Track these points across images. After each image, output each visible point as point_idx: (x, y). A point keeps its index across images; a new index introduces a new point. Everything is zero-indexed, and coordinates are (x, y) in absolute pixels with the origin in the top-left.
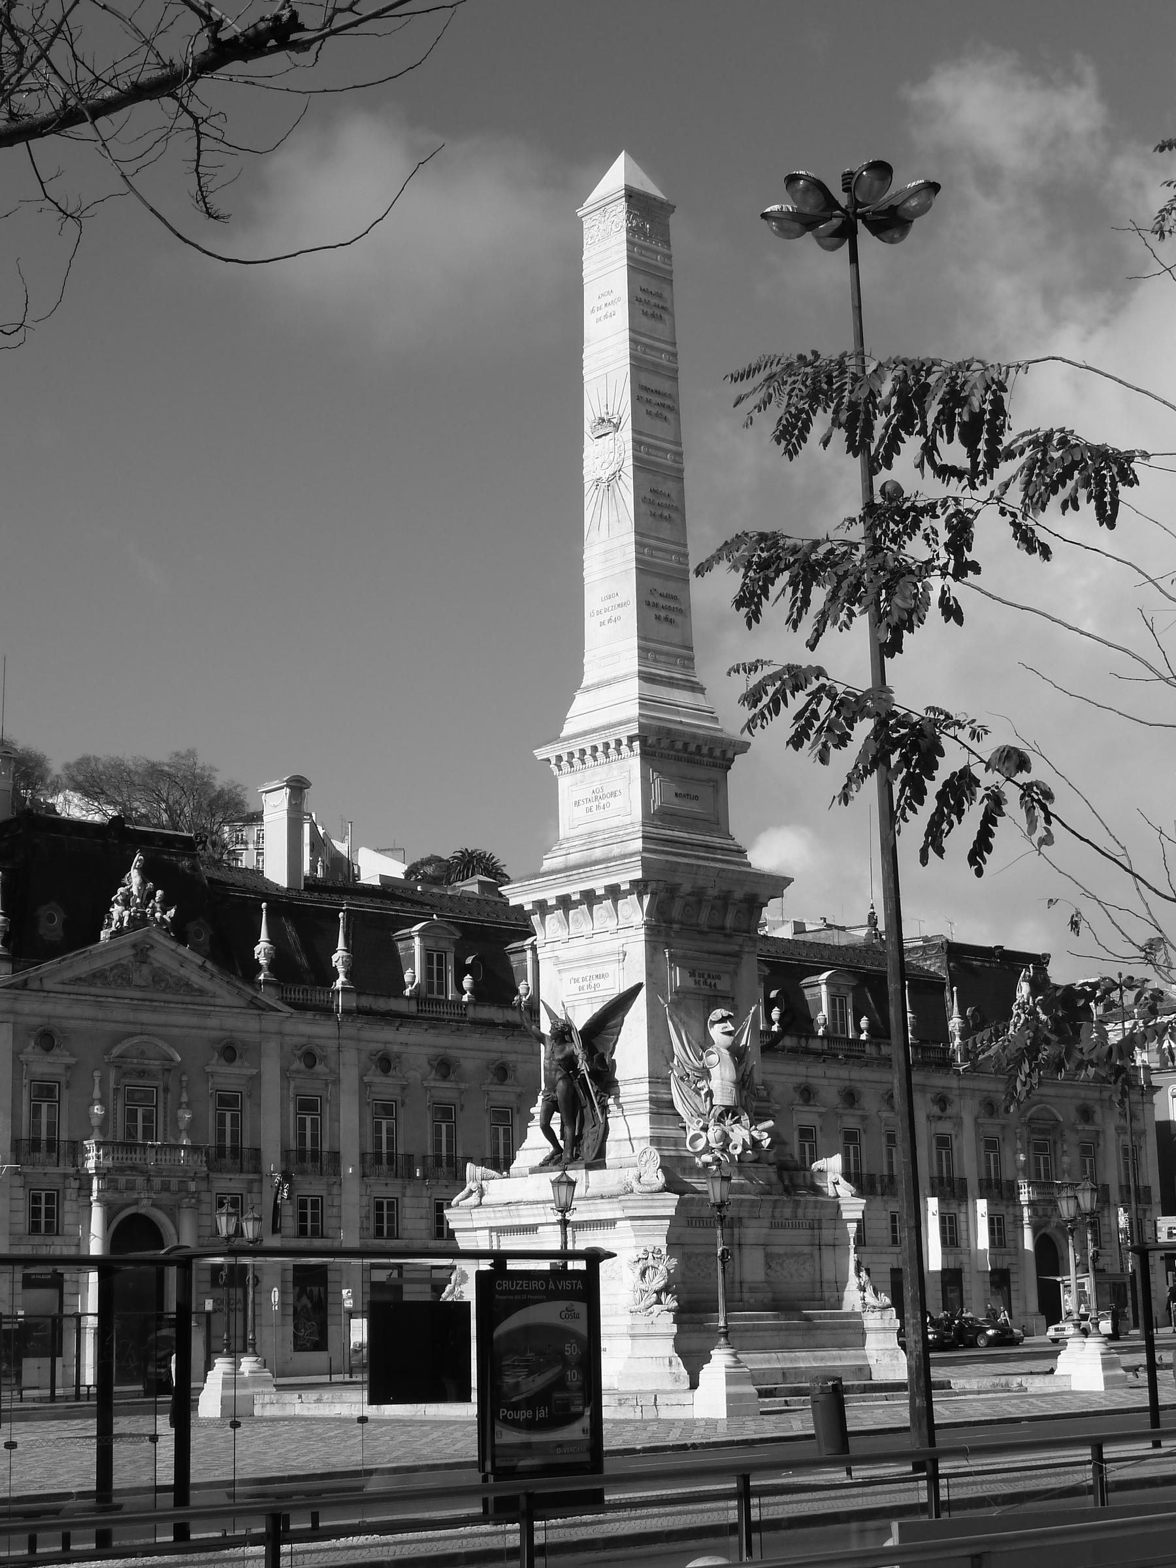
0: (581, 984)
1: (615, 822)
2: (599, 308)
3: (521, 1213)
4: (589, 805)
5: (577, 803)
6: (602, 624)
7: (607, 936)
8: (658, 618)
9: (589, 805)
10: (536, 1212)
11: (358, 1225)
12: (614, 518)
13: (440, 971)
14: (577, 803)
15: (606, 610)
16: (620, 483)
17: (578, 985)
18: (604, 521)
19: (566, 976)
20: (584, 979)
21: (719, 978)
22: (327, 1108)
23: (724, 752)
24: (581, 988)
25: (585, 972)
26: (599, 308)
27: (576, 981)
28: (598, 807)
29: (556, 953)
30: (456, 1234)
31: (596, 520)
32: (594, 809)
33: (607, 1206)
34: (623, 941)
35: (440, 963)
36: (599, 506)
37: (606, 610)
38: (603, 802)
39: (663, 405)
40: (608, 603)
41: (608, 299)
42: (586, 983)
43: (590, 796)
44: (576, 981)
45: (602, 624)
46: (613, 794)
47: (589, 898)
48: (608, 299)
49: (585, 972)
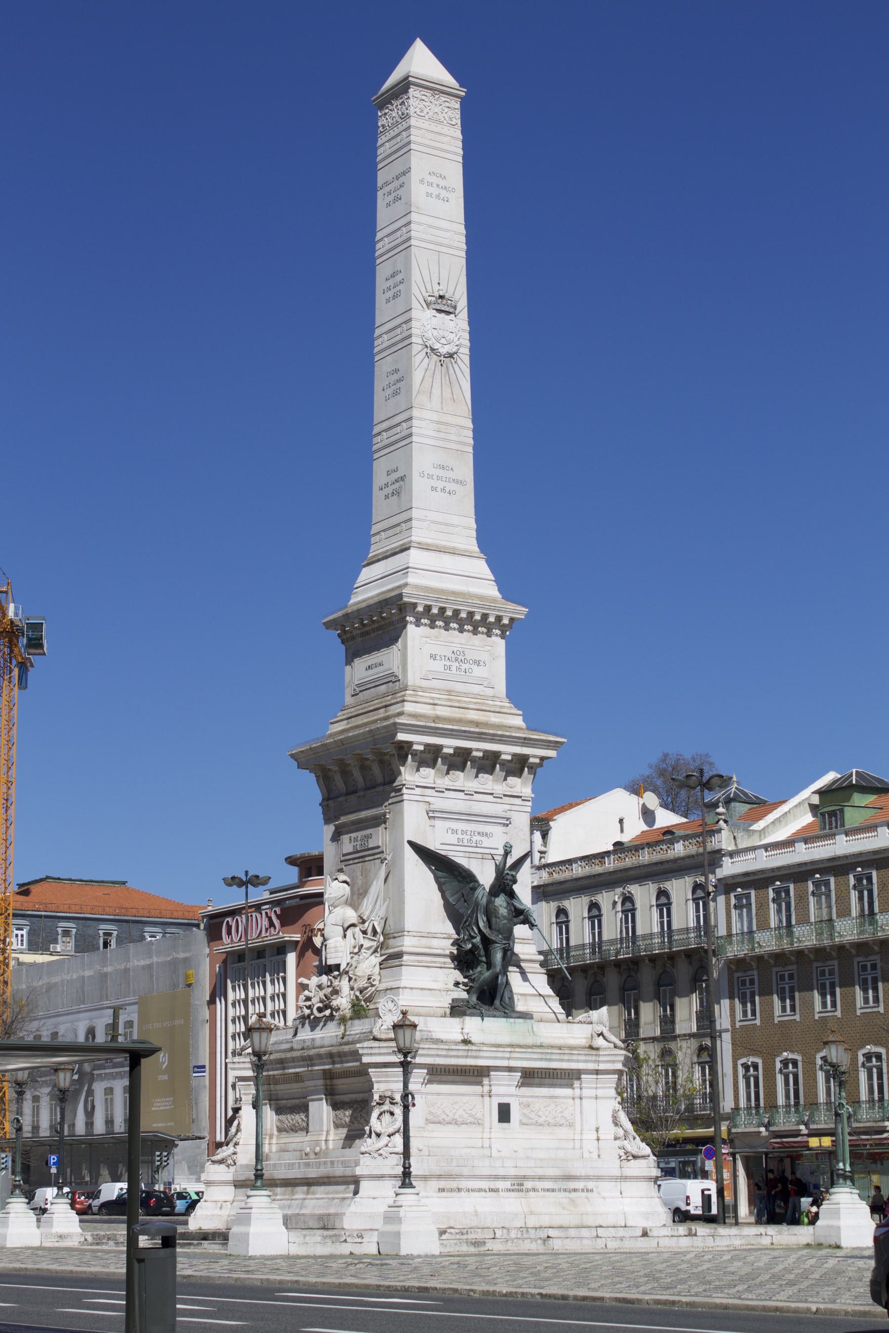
0: (461, 837)
1: (476, 689)
3: (481, 1054)
4: (448, 663)
5: (433, 657)
6: (434, 489)
7: (490, 798)
9: (448, 663)
10: (500, 1055)
12: (447, 393)
14: (433, 657)
15: (439, 478)
16: (455, 366)
18: (436, 391)
19: (438, 823)
27: (454, 832)
28: (458, 669)
32: (454, 668)
33: (583, 1058)
34: (508, 807)
36: (430, 373)
37: (439, 478)
38: (464, 666)
40: (440, 472)
41: (442, 183)
43: (449, 655)
44: (454, 832)
45: (434, 489)
46: (477, 663)
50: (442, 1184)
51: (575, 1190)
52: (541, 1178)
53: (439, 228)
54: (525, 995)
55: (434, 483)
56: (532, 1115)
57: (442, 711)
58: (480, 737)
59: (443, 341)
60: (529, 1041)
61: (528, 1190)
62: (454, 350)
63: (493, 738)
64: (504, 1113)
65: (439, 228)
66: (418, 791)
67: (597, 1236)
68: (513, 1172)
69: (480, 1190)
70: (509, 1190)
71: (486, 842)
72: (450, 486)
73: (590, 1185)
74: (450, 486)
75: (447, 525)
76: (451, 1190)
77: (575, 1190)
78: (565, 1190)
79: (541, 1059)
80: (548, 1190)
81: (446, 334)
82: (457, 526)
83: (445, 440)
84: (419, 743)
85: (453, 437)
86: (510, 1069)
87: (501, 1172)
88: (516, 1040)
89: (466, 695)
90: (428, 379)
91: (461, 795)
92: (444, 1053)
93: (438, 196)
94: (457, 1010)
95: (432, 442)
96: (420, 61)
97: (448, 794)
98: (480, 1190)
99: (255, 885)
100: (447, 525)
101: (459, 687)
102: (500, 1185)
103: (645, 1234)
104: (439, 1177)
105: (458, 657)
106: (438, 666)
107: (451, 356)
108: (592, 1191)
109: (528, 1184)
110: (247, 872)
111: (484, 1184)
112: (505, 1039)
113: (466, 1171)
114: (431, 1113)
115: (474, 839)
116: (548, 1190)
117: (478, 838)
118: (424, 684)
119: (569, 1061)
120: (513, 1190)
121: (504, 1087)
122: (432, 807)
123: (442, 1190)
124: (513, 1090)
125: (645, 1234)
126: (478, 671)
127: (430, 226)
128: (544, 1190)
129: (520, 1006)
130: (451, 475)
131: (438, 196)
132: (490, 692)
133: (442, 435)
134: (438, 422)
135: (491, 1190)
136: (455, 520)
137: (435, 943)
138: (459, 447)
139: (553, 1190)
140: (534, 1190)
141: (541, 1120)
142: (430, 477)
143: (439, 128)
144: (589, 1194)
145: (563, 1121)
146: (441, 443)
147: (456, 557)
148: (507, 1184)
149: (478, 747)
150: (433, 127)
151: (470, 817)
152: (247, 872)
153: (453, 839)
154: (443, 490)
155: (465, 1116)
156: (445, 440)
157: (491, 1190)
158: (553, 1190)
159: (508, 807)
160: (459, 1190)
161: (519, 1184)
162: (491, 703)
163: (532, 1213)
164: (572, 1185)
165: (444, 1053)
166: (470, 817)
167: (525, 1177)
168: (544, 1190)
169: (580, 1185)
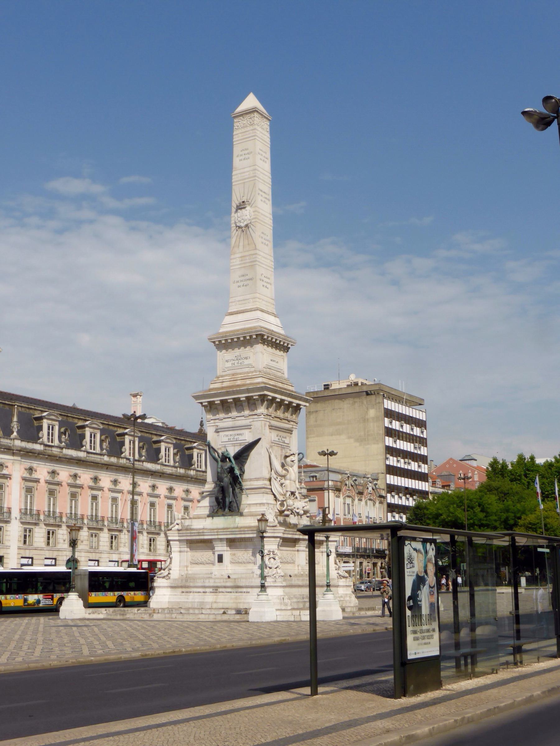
0: (229, 437)
1: (247, 370)
2: (242, 155)
4: (233, 362)
5: (227, 361)
6: (239, 286)
7: (243, 418)
8: (263, 286)
9: (233, 362)
11: (17, 539)
12: (246, 242)
13: (52, 434)
14: (227, 361)
15: (241, 281)
17: (227, 438)
18: (241, 244)
19: (221, 434)
21: (286, 438)
22: (7, 489)
23: (288, 344)
26: (242, 155)
27: (227, 436)
28: (238, 363)
29: (217, 424)
30: (171, 542)
32: (236, 364)
34: (252, 420)
35: (52, 430)
37: (241, 281)
38: (240, 361)
39: (266, 198)
40: (242, 278)
41: (246, 152)
42: (232, 437)
43: (234, 358)
44: (227, 436)
46: (246, 358)
47: (237, 402)
48: (246, 152)
50: (184, 590)
51: (241, 592)
52: (225, 587)
53: (244, 173)
54: (249, 504)
56: (236, 559)
57: (225, 384)
58: (228, 393)
59: (242, 221)
60: (232, 526)
61: (220, 592)
62: (249, 222)
63: (234, 393)
64: (220, 559)
65: (244, 173)
66: (212, 421)
67: (202, 613)
68: (212, 584)
69: (199, 592)
70: (211, 592)
71: (241, 438)
72: (245, 283)
73: (249, 590)
74: (245, 283)
75: (244, 300)
76: (187, 592)
77: (241, 592)
78: (236, 592)
79: (232, 534)
80: (228, 592)
81: (243, 217)
82: (248, 299)
83: (244, 263)
84: (217, 401)
85: (248, 261)
86: (221, 540)
87: (207, 584)
88: (225, 526)
89: (241, 374)
90: (238, 240)
91: (230, 419)
92: (189, 534)
93: (244, 159)
94: (212, 514)
95: (239, 266)
96: (251, 101)
97: (224, 420)
98: (199, 592)
99: (331, 455)
100: (244, 300)
101: (239, 371)
102: (208, 590)
103: (224, 613)
104: (182, 587)
105: (238, 358)
106: (229, 365)
107: (247, 226)
108: (249, 592)
109: (220, 590)
110: (328, 450)
111: (201, 590)
112: (221, 526)
113: (192, 584)
114: (192, 560)
115: (235, 437)
116: (228, 592)
117: (237, 437)
118: (224, 374)
119: (244, 534)
120: (213, 592)
121: (221, 548)
122: (219, 427)
123: (183, 592)
124: (225, 548)
125: (224, 613)
126: (246, 362)
127: (240, 174)
128: (227, 592)
129: (246, 511)
130: (247, 277)
131: (244, 159)
132: (253, 369)
133: (242, 262)
134: (241, 257)
135: (204, 592)
136: (248, 297)
138: (250, 264)
139: (231, 592)
140: (222, 592)
141: (240, 561)
142: (238, 282)
143: (246, 129)
144: (248, 594)
145: (250, 561)
146: (243, 266)
147: (245, 314)
148: (211, 590)
149: (230, 398)
150: (243, 130)
151: (233, 428)
152: (328, 450)
153: (226, 439)
155: (207, 560)
156: (244, 263)
157: (204, 592)
158: (231, 592)
159: (252, 420)
160: (190, 592)
161: (216, 589)
163: (215, 602)
164: (240, 590)
165: (189, 534)
166: (233, 428)
167: (218, 587)
168: (227, 592)
169: (245, 590)
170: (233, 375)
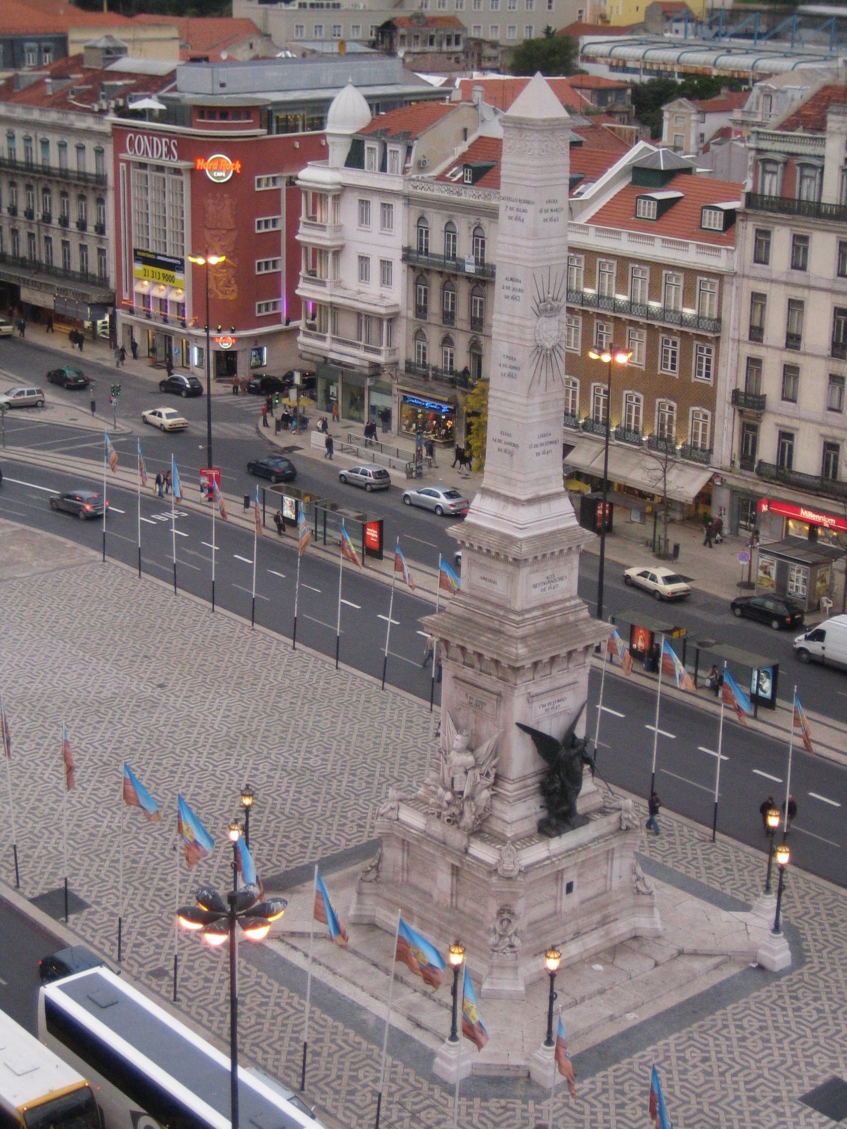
2: (546, 211)
5: (535, 586)
6: (538, 454)
15: (542, 445)
18: (543, 379)
19: (536, 705)
20: (549, 704)
24: (547, 710)
25: (550, 700)
26: (546, 211)
27: (544, 706)
31: (537, 377)
37: (542, 445)
40: (543, 440)
44: (544, 706)
45: (538, 454)
46: (561, 579)
49: (550, 700)
55: (537, 450)
71: (562, 704)
90: (538, 371)
105: (550, 580)
137: (529, 781)
142: (536, 446)
154: (544, 453)
162: (568, 604)
170: (543, 606)
